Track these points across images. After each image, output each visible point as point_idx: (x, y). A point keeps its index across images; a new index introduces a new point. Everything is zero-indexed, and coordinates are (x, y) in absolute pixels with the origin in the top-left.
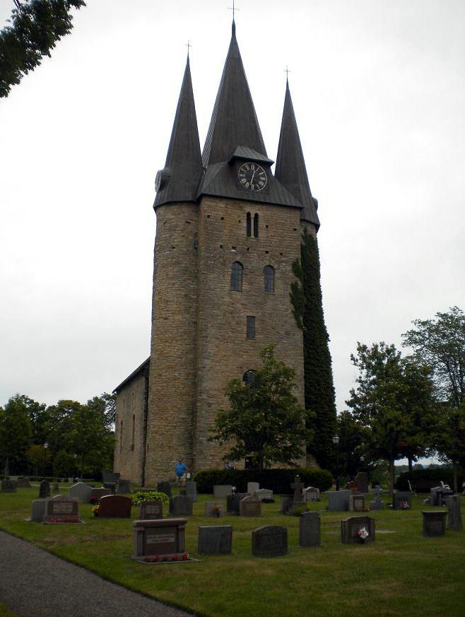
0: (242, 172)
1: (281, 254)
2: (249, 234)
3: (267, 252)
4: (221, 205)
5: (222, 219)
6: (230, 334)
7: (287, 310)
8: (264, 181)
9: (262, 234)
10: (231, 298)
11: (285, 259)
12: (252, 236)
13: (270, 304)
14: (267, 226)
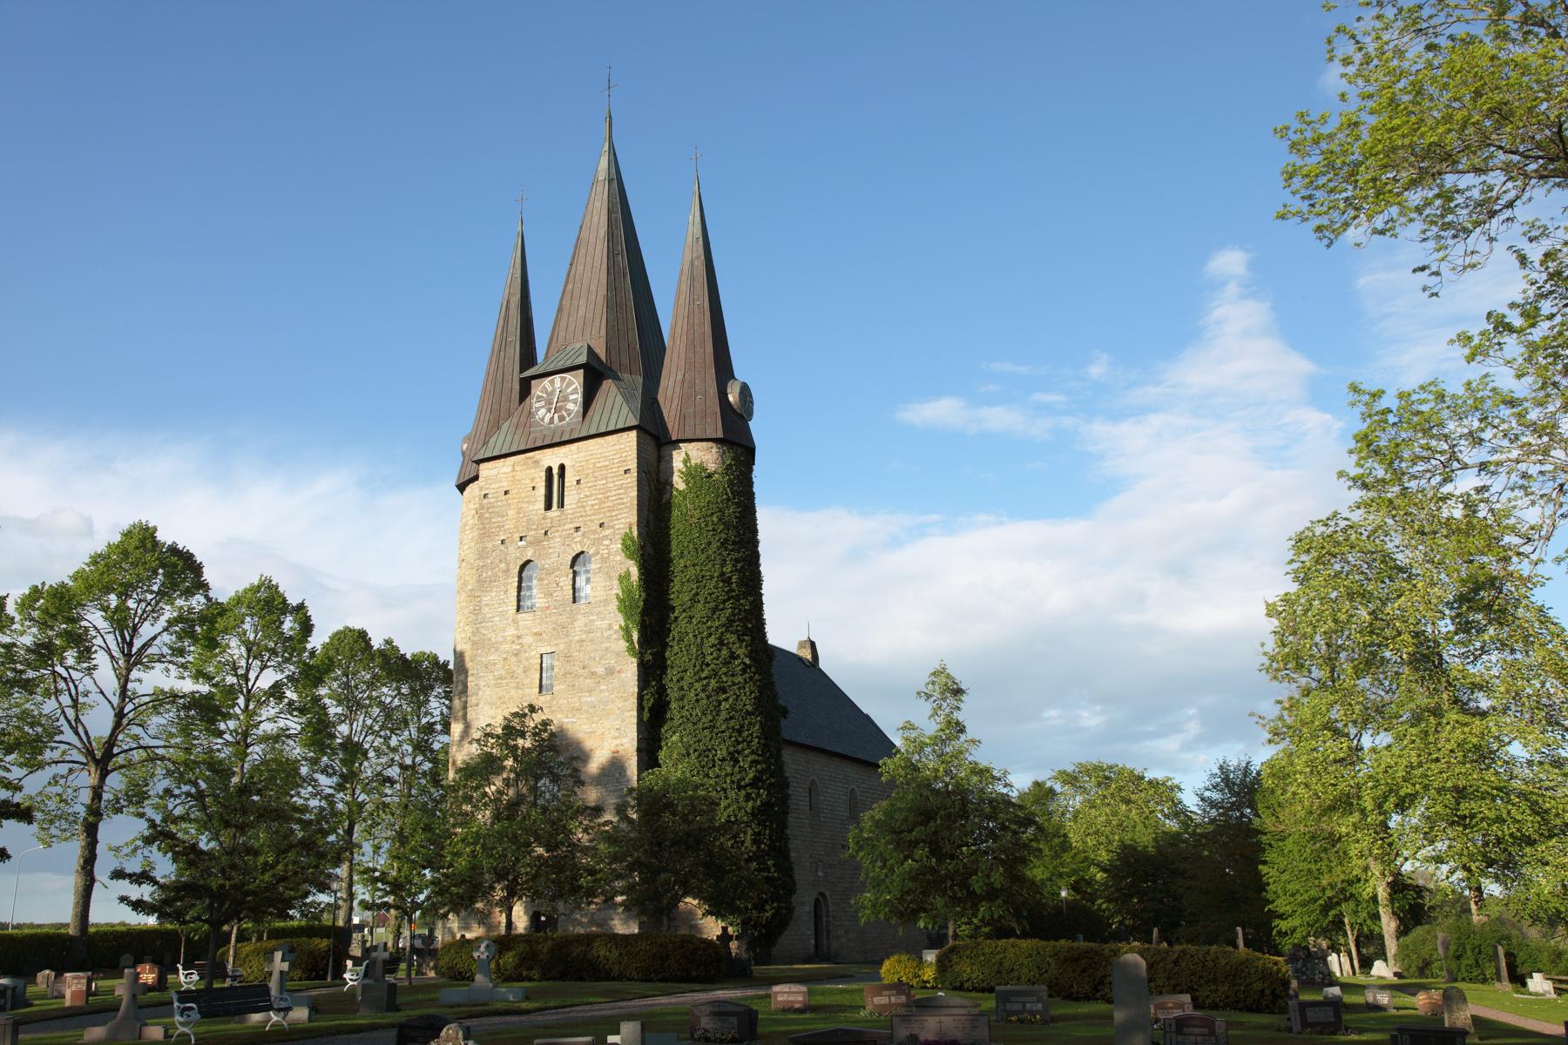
2: (548, 506)
6: (513, 692)
11: (607, 532)
13: (581, 622)
14: (578, 482)
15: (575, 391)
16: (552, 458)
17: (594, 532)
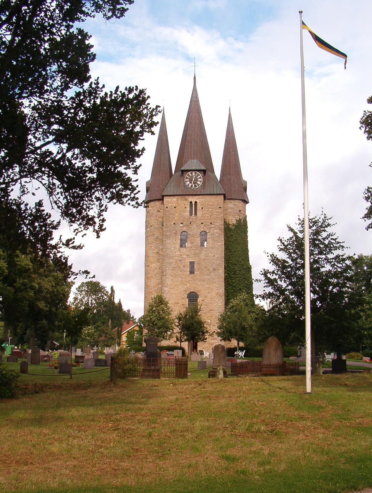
0: (187, 178)
1: (211, 223)
3: (202, 223)
4: (174, 199)
5: (175, 207)
6: (180, 273)
7: (214, 256)
8: (200, 181)
9: (199, 213)
10: (180, 252)
12: (193, 215)
13: (204, 253)
15: (200, 178)
16: (193, 199)
17: (209, 225)
